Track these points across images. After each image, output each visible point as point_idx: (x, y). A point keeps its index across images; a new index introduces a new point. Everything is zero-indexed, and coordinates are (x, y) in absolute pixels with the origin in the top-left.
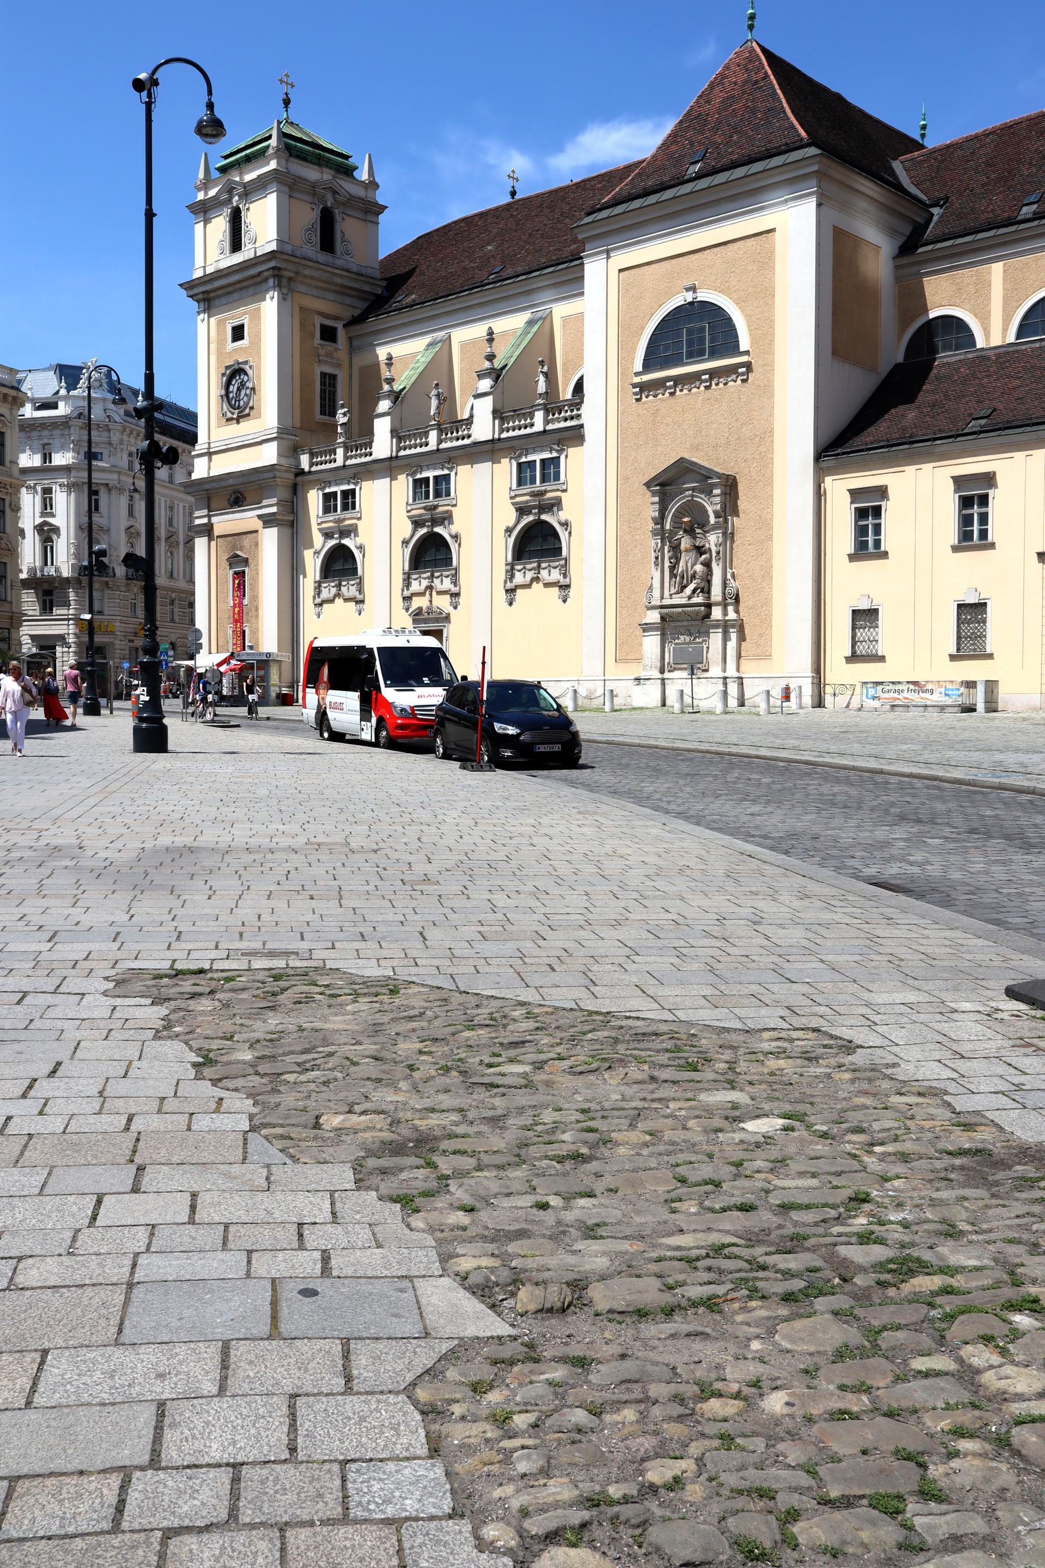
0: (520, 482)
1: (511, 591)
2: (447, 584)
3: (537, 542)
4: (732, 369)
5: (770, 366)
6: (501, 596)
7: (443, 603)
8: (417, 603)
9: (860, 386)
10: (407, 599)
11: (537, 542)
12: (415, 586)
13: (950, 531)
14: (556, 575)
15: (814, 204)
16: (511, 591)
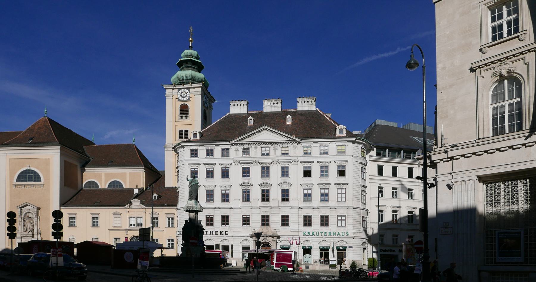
4: (41, 185)
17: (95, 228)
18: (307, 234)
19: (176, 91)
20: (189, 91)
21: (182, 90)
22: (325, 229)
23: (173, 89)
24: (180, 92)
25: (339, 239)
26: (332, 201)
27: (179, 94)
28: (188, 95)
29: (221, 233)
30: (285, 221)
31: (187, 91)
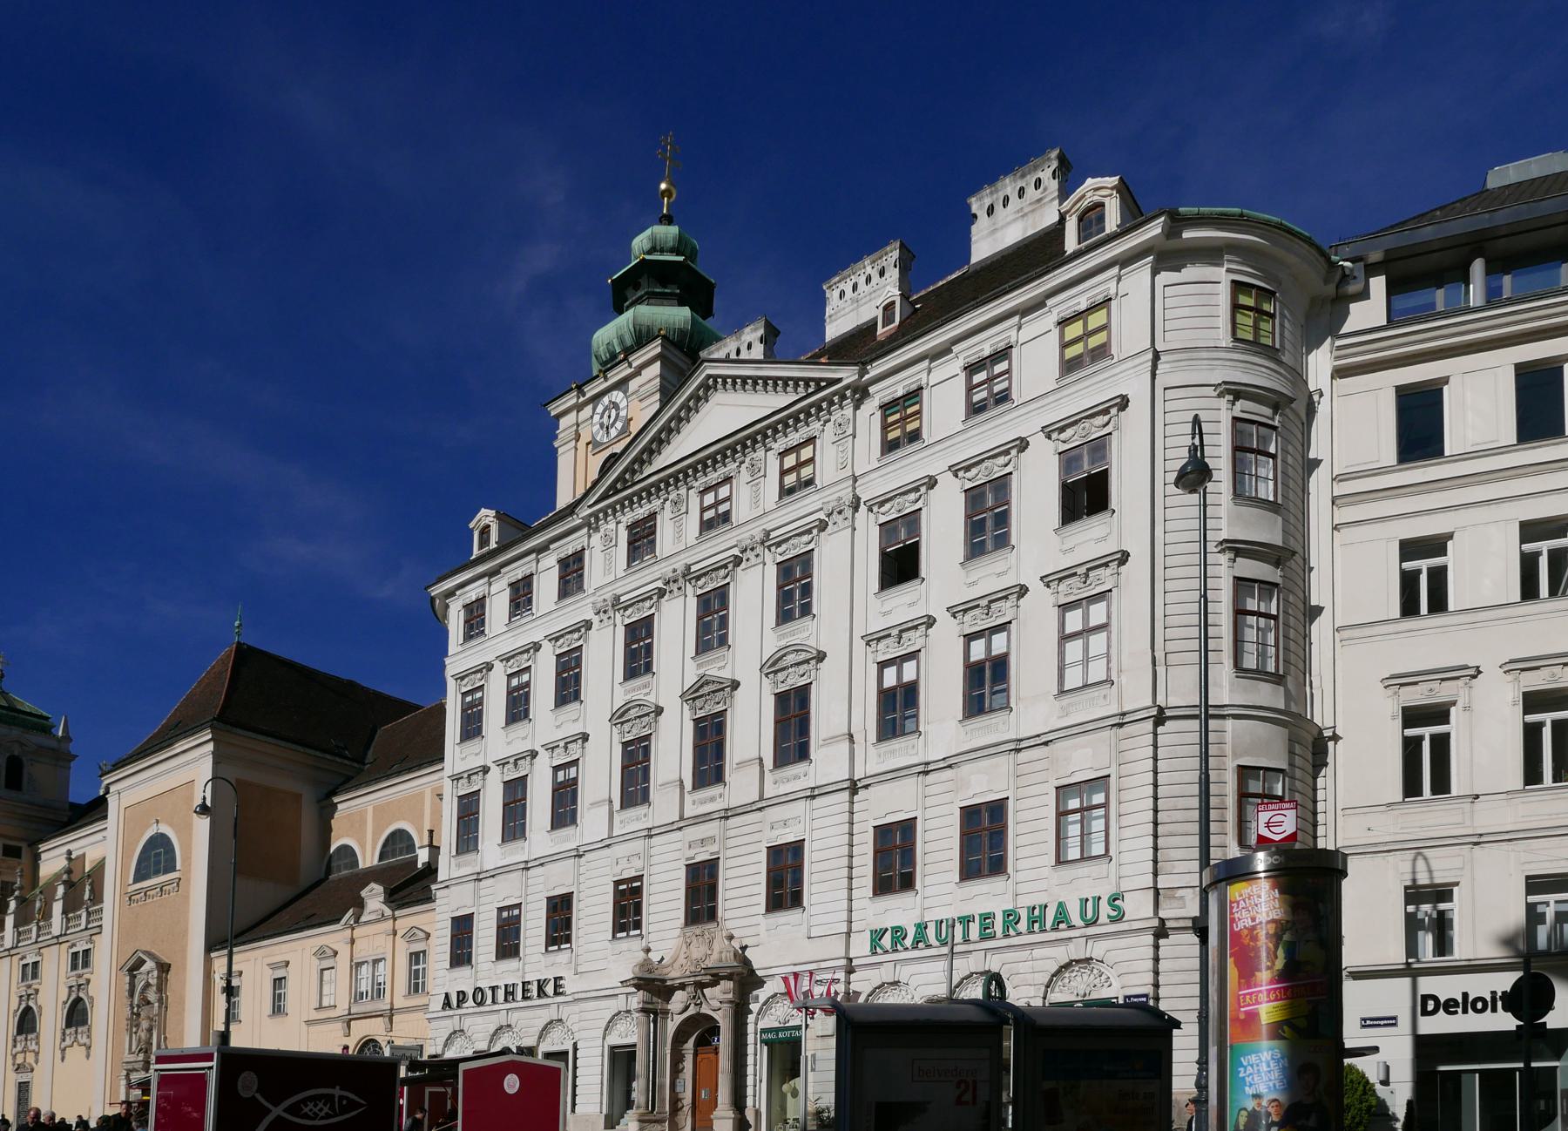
0: (74, 967)
1: (63, 1050)
2: (33, 1047)
3: (77, 1014)
4: (170, 883)
5: (188, 880)
6: (58, 1054)
7: (30, 1058)
8: (20, 1060)
9: (267, 894)
10: (14, 1057)
11: (77, 1014)
12: (19, 1048)
13: (268, 1008)
14: (84, 1040)
15: (209, 761)
16: (63, 1050)
17: (279, 1019)
18: (887, 941)
19: (588, 410)
20: (625, 392)
21: (606, 400)
22: (989, 896)
23: (579, 408)
24: (600, 409)
25: (1062, 954)
26: (1032, 703)
27: (597, 418)
28: (623, 413)
29: (541, 992)
30: (785, 882)
31: (617, 396)
